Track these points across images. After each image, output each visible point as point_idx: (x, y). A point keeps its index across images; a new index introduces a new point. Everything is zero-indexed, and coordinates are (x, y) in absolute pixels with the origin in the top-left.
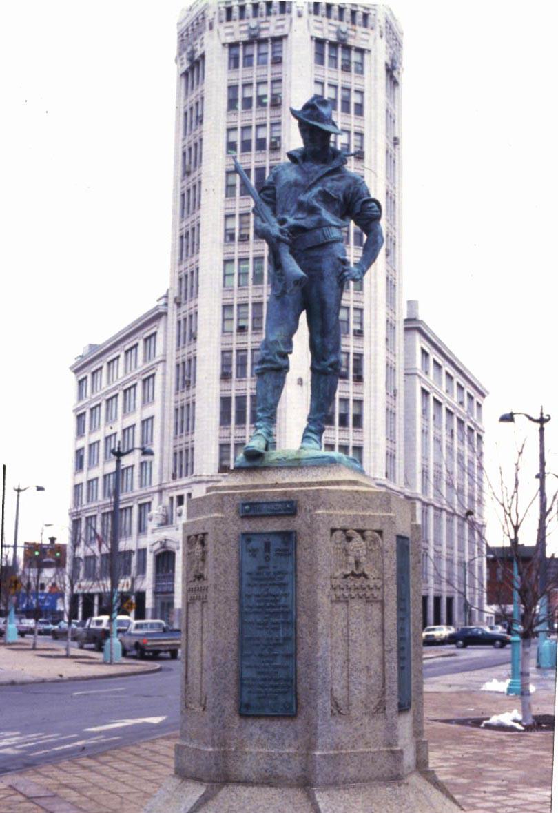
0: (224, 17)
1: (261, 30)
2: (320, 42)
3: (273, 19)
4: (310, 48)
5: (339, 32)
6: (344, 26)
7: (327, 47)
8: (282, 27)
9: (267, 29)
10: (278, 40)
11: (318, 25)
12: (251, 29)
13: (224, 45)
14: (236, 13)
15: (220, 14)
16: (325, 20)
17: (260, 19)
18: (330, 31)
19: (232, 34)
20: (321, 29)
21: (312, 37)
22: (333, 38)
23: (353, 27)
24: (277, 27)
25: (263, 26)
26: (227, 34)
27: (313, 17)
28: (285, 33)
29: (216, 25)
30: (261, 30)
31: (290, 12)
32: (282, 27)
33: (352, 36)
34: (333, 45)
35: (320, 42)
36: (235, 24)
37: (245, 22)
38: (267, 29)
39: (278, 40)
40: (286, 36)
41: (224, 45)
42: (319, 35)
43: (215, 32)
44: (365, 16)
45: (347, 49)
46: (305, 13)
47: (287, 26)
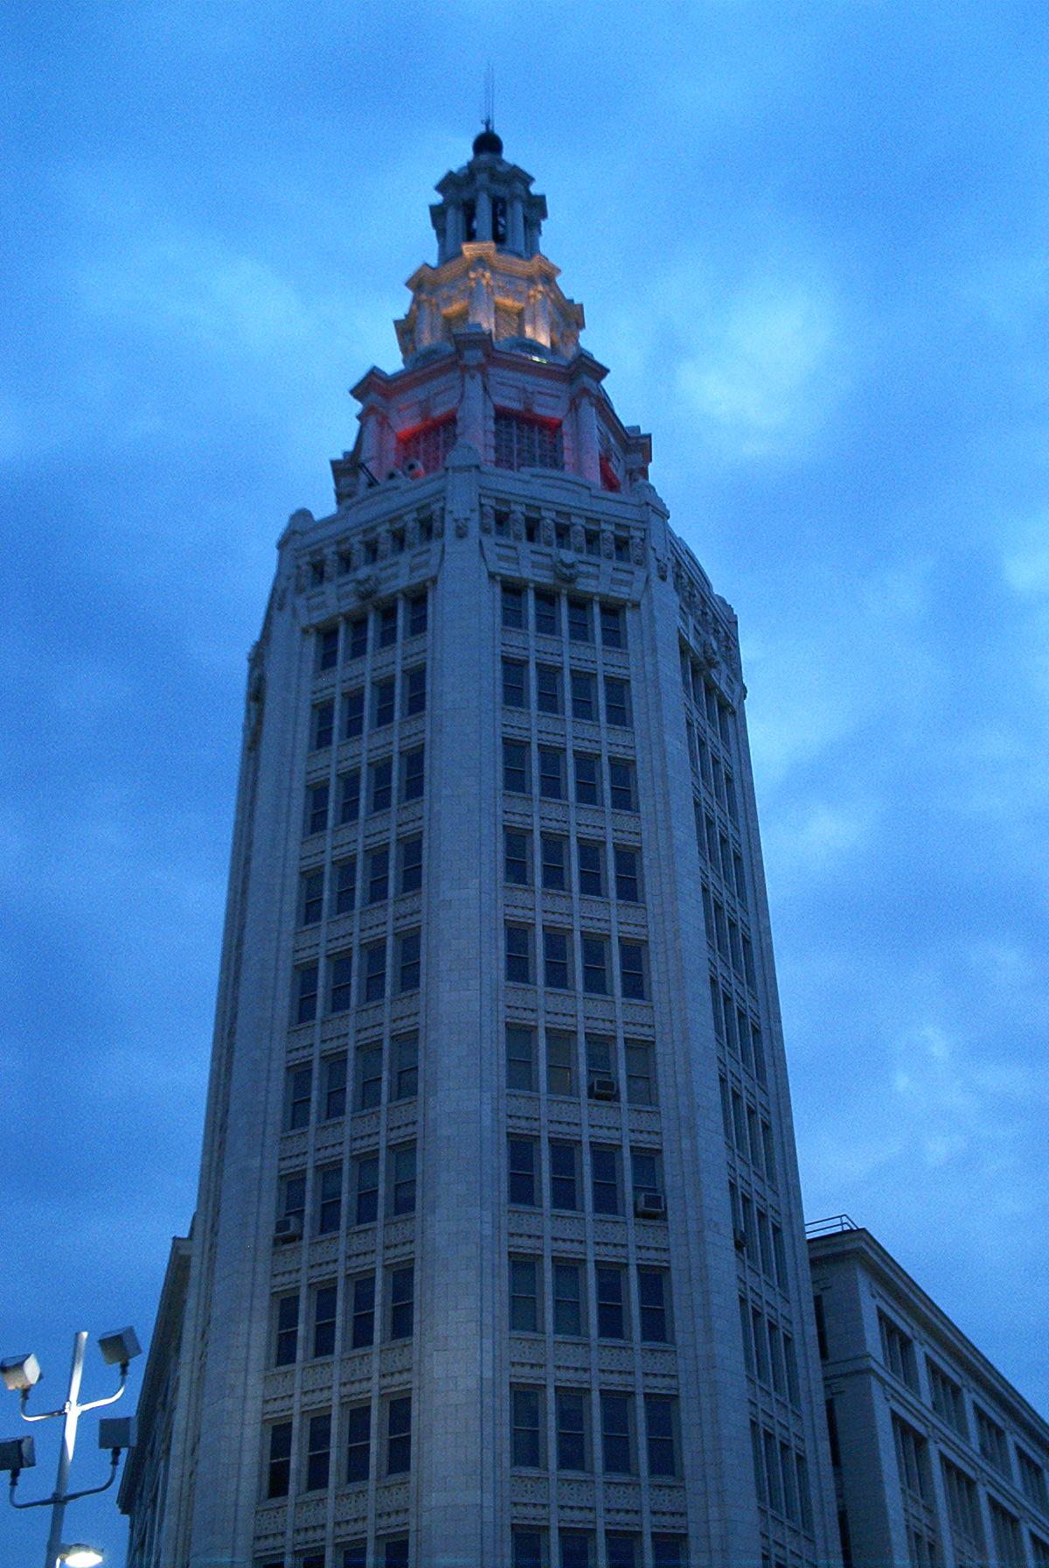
1: (378, 582)
2: (512, 590)
3: (405, 558)
4: (490, 600)
5: (558, 568)
6: (568, 556)
7: (531, 597)
12: (359, 582)
13: (305, 631)
16: (525, 547)
17: (380, 564)
19: (323, 605)
21: (492, 576)
22: (545, 578)
23: (593, 559)
25: (384, 574)
28: (432, 573)
30: (378, 582)
31: (441, 534)
33: (588, 575)
34: (546, 597)
35: (512, 590)
36: (329, 589)
37: (351, 576)
38: (396, 576)
39: (418, 599)
41: (305, 631)
42: (506, 569)
43: (288, 610)
44: (622, 545)
45: (579, 604)
46: (474, 529)
47: (434, 561)
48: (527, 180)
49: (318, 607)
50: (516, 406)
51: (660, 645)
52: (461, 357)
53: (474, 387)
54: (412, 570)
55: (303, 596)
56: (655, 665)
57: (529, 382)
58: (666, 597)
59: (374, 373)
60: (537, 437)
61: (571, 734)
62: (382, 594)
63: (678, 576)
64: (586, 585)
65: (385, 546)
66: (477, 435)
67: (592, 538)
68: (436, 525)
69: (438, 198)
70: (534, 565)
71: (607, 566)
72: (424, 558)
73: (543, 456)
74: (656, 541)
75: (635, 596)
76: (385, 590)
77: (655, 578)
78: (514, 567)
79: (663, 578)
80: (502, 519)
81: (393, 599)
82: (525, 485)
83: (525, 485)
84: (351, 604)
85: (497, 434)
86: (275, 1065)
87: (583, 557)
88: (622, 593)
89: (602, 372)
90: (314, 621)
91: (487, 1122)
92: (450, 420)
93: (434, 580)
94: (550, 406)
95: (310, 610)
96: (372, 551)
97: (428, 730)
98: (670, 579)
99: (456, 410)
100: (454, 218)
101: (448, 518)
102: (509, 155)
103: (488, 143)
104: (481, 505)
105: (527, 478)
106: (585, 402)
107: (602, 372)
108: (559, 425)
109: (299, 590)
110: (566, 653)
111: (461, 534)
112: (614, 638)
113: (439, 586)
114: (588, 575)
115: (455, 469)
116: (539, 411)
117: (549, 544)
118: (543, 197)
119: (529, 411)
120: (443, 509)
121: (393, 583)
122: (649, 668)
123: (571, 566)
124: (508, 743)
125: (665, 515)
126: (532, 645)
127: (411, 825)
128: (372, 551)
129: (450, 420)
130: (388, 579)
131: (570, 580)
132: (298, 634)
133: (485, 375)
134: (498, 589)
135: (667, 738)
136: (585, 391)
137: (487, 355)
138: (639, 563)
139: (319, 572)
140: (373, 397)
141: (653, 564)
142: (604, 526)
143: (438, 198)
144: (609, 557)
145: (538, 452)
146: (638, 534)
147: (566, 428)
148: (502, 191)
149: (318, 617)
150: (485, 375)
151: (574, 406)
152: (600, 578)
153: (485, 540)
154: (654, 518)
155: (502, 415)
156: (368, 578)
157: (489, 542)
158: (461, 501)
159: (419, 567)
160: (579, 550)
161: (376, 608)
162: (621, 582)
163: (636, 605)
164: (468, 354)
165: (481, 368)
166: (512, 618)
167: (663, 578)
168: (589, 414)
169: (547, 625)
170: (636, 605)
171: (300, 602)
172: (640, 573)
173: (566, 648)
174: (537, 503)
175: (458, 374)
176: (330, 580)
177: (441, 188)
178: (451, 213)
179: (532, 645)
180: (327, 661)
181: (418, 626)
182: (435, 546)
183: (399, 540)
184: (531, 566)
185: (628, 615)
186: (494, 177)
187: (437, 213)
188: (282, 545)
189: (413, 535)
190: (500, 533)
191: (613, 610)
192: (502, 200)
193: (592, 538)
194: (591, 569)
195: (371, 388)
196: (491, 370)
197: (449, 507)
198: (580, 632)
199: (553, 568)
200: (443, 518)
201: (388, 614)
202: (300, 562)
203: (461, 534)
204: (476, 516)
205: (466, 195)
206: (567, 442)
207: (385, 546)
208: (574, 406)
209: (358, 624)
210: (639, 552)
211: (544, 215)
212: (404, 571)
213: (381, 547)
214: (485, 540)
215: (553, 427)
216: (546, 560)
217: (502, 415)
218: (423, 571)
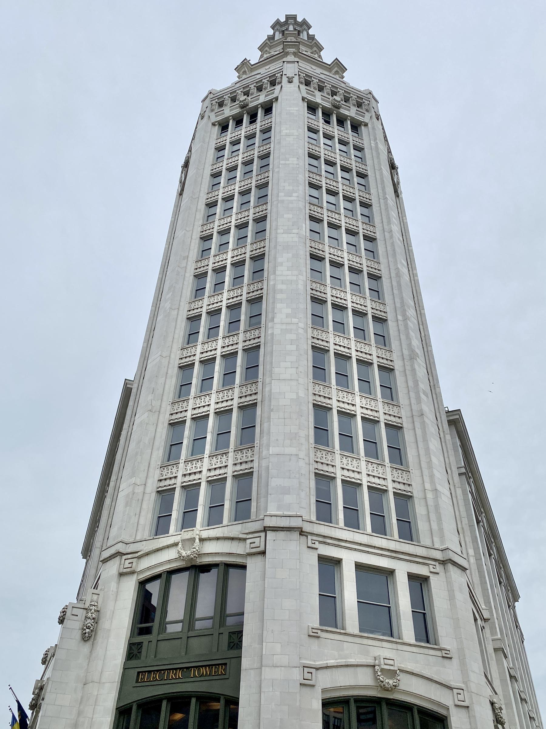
12: (241, 102)
20: (314, 96)
21: (303, 99)
22: (328, 105)
24: (266, 96)
26: (216, 116)
27: (303, 87)
35: (312, 108)
39: (268, 109)
48: (309, 27)
59: (245, 62)
69: (271, 32)
76: (251, 105)
81: (256, 108)
86: (187, 275)
88: (361, 119)
91: (301, 287)
93: (277, 99)
111: (290, 81)
117: (328, 94)
120: (282, 75)
123: (339, 102)
131: (338, 107)
134: (306, 104)
138: (367, 111)
144: (354, 105)
146: (367, 102)
149: (219, 118)
153: (300, 85)
161: (248, 113)
177: (273, 27)
182: (278, 87)
195: (244, 67)
201: (253, 118)
203: (290, 81)
214: (300, 85)
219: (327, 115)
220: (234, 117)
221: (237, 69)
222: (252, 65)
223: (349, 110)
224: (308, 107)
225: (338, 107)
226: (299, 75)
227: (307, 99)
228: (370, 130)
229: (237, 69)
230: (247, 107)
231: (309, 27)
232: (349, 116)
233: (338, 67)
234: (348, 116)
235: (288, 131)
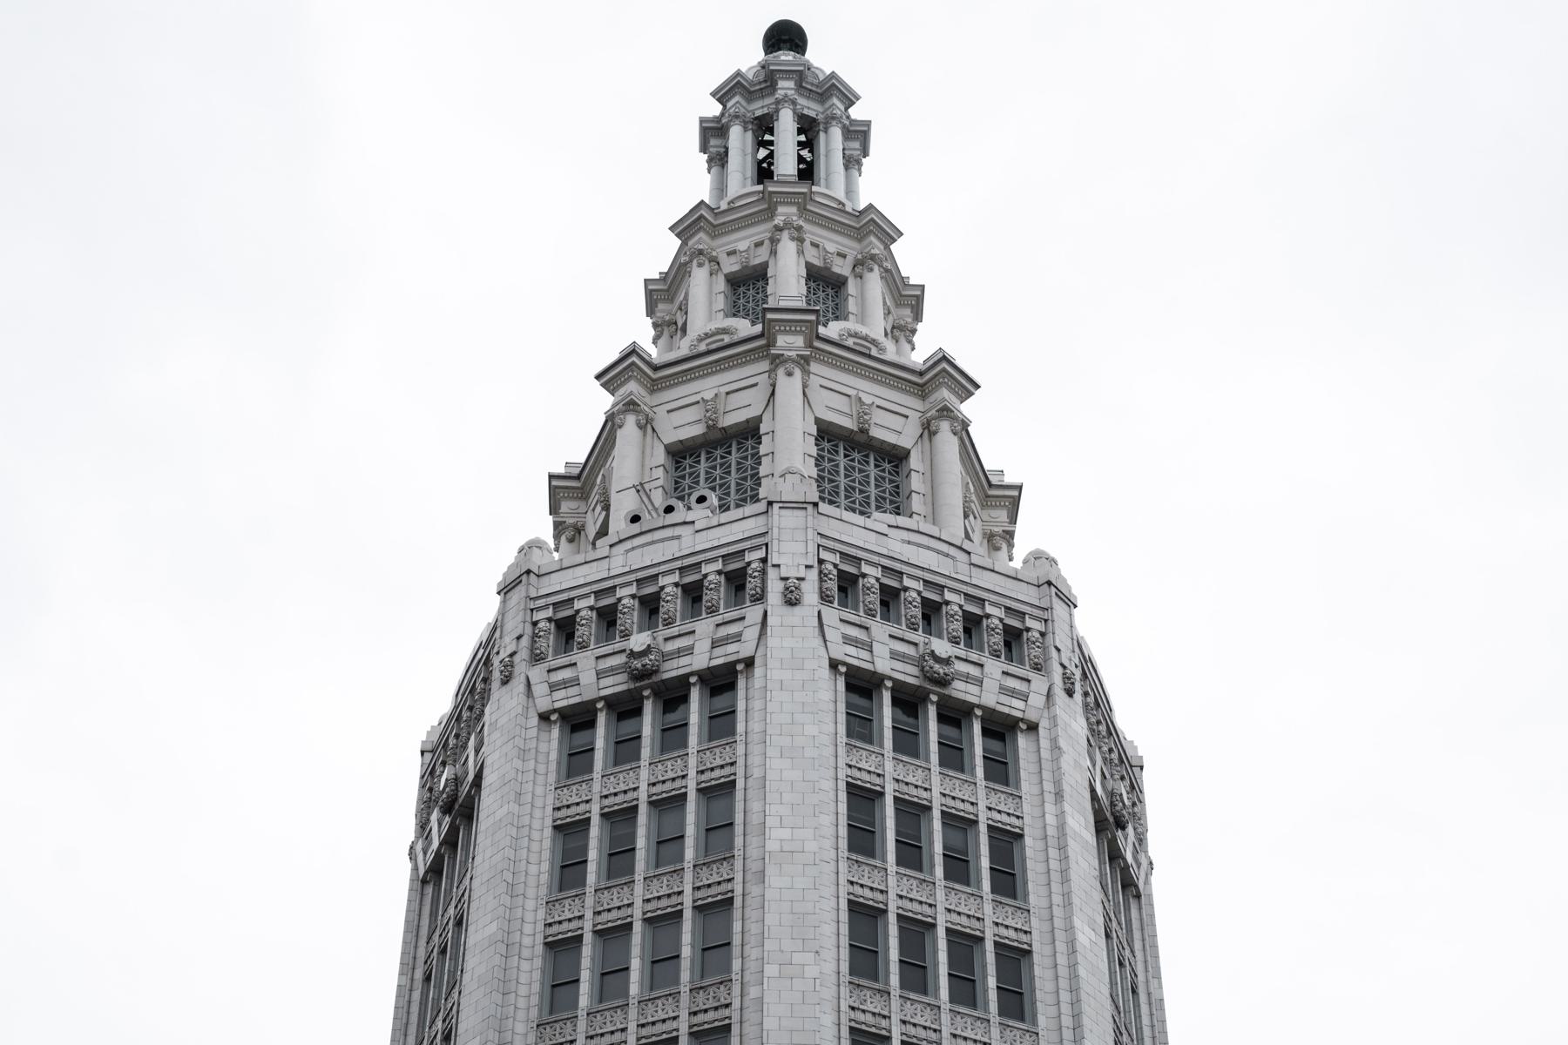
0: (548, 643)
1: (666, 657)
2: (861, 685)
3: (704, 627)
4: (829, 695)
6: (942, 647)
7: (887, 697)
8: (737, 638)
9: (689, 650)
10: (721, 681)
11: (854, 632)
12: (633, 655)
13: (544, 717)
14: (587, 629)
15: (535, 636)
18: (895, 655)
19: (575, 682)
21: (834, 665)
22: (908, 674)
26: (554, 687)
28: (745, 649)
29: (521, 668)
31: (760, 598)
32: (737, 638)
33: (967, 678)
34: (908, 702)
35: (861, 685)
39: (721, 681)
40: (749, 663)
41: (544, 717)
42: (855, 657)
43: (518, 685)
45: (955, 715)
47: (751, 634)
48: (850, 99)
49: (565, 684)
50: (848, 423)
51: (1066, 787)
52: (771, 343)
53: (790, 387)
54: (715, 644)
55: (545, 666)
56: (1061, 816)
57: (870, 391)
58: (1072, 721)
60: (872, 471)
61: (945, 906)
62: (666, 676)
63: (1086, 694)
64: (962, 691)
65: (673, 603)
66: (790, 452)
67: (972, 624)
68: (752, 584)
69: (715, 109)
70: (895, 655)
71: (994, 667)
72: (732, 629)
73: (850, 490)
74: (1062, 639)
75: (1032, 716)
76: (672, 670)
77: (1059, 690)
78: (865, 655)
79: (1070, 693)
80: (847, 585)
81: (683, 683)
82: (872, 535)
83: (872, 535)
84: (615, 685)
85: (819, 461)
87: (962, 654)
88: (1014, 707)
89: (966, 386)
90: (558, 705)
92: (750, 432)
93: (749, 663)
94: (894, 424)
95: (554, 687)
96: (650, 606)
97: (739, 877)
98: (1078, 696)
99: (759, 419)
100: (739, 140)
101: (772, 574)
102: (820, 56)
103: (785, 37)
104: (821, 562)
105: (884, 529)
106: (945, 426)
107: (966, 386)
108: (908, 452)
109: (536, 658)
110: (937, 787)
111: (792, 599)
112: (1001, 771)
113: (758, 671)
114: (967, 678)
115: (787, 505)
116: (876, 433)
117: (913, 627)
118: (868, 124)
119: (864, 431)
120: (764, 560)
121: (684, 661)
122: (1050, 819)
123: (947, 662)
124: (855, 907)
125: (1070, 603)
126: (890, 772)
127: (711, 1015)
128: (650, 606)
129: (750, 432)
130: (680, 653)
131: (944, 682)
132: (535, 720)
133: (806, 373)
135: (1077, 922)
136: (946, 412)
137: (810, 345)
138: (1037, 668)
139: (566, 629)
140: (632, 387)
141: (1057, 673)
142: (989, 609)
143: (715, 109)
144: (995, 654)
145: (842, 481)
147: (915, 462)
148: (812, 108)
149: (564, 699)
150: (806, 373)
151: (928, 430)
152: (986, 683)
154: (1059, 606)
155: (826, 433)
156: (647, 651)
157: (832, 615)
158: (793, 547)
159: (727, 640)
160: (955, 641)
162: (1013, 693)
163: (1033, 727)
164: (782, 340)
165: (803, 362)
166: (860, 727)
167: (1070, 693)
168: (947, 443)
169: (908, 743)
170: (1033, 727)
171: (537, 674)
172: (1039, 684)
173: (936, 779)
174: (897, 566)
175: (764, 365)
176: (583, 646)
177: (722, 95)
178: (735, 132)
179: (890, 772)
180: (576, 763)
181: (722, 724)
182: (753, 613)
183: (693, 594)
184: (888, 652)
185: (1023, 741)
186: (800, 87)
187: (712, 134)
188: (506, 590)
189: (715, 591)
190: (844, 604)
191: (1001, 728)
192: (813, 121)
193: (972, 624)
194: (974, 671)
196: (814, 367)
197: (774, 558)
198: (953, 757)
199: (920, 662)
200: (764, 572)
202: (538, 616)
203: (792, 599)
204: (813, 575)
205: (759, 108)
206: (916, 482)
207: (673, 603)
208: (928, 430)
209: (625, 708)
210: (1036, 652)
211: (865, 152)
212: (702, 647)
213: (664, 607)
214: (826, 611)
215: (895, 458)
216: (910, 650)
217: (826, 433)
218: (731, 648)
219: (908, 702)
220: (612, 703)
221: (610, 378)
222: (656, 368)
223: (979, 682)
224: (850, 687)
225: (944, 682)
226: (821, 562)
227: (844, 664)
228: (1045, 743)
229: (610, 378)
230: (655, 679)
231: (850, 99)
232: (979, 706)
233: (946, 378)
234: (972, 706)
235: (785, 834)
